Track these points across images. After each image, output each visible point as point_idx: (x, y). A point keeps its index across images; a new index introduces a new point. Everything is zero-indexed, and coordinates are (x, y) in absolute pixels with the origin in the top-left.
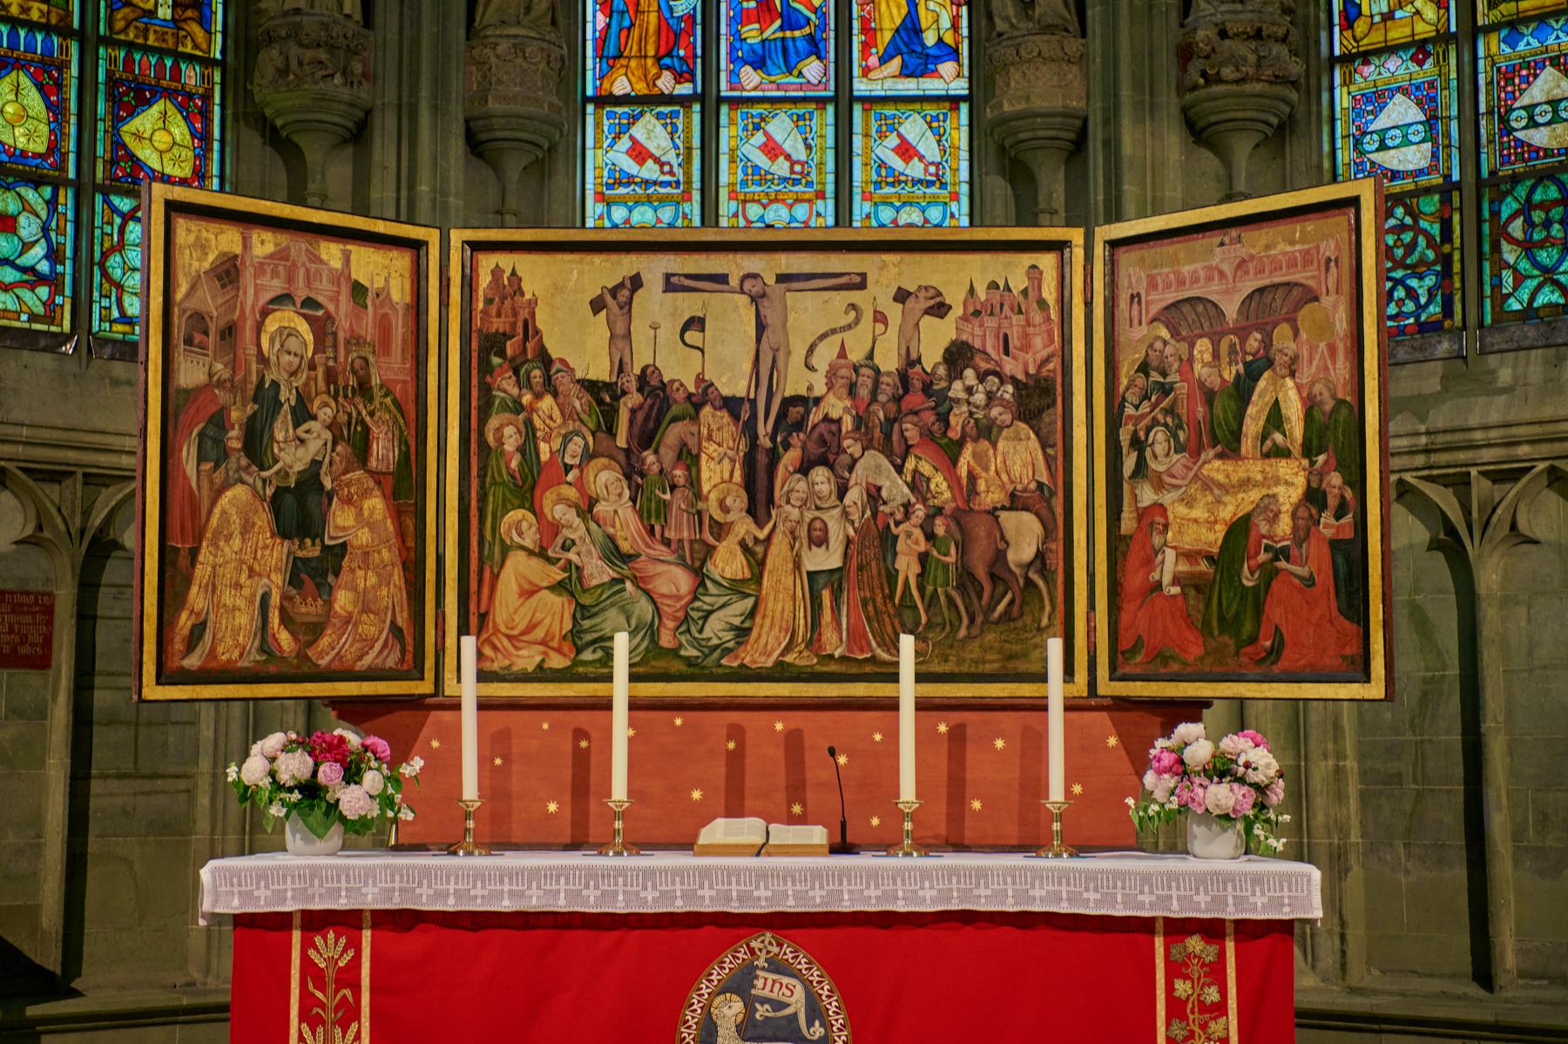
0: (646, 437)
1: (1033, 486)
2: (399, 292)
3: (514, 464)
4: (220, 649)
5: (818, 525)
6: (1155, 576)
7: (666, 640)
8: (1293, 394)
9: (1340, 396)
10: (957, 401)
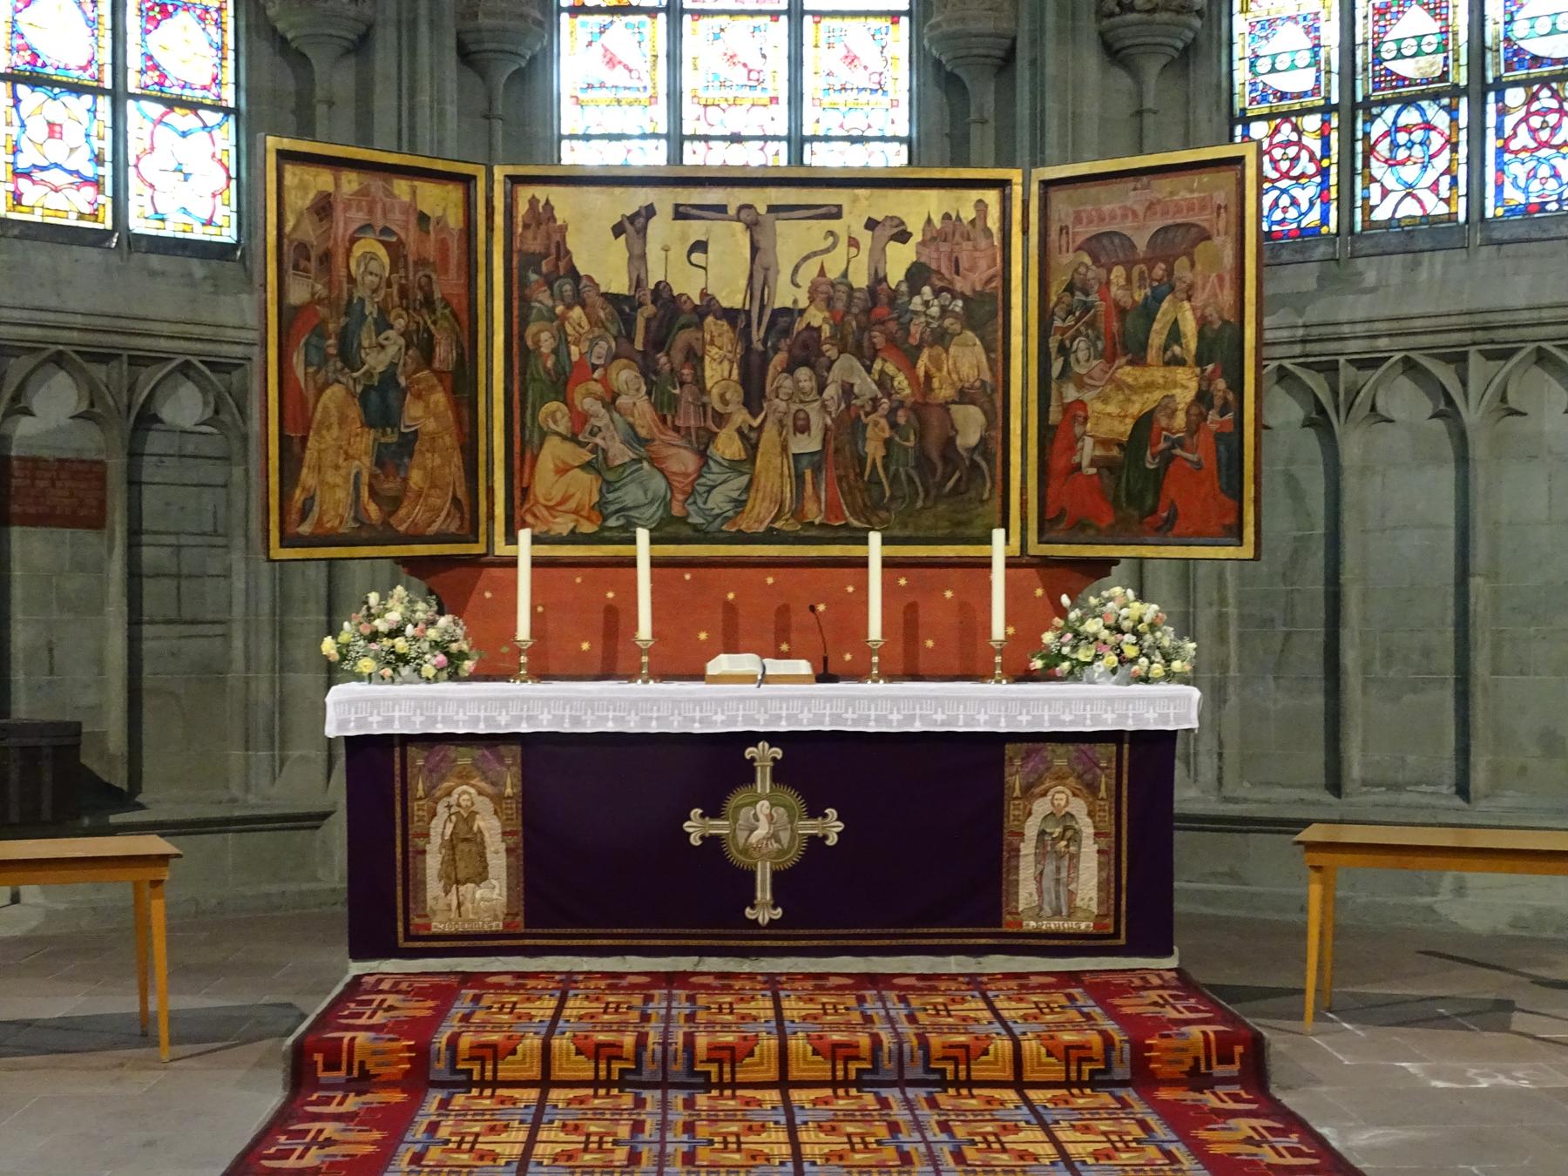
0: (658, 342)
1: (978, 384)
2: (455, 220)
3: (549, 364)
4: (325, 519)
5: (802, 415)
6: (1076, 459)
7: (677, 510)
8: (1189, 315)
9: (1226, 317)
10: (915, 313)
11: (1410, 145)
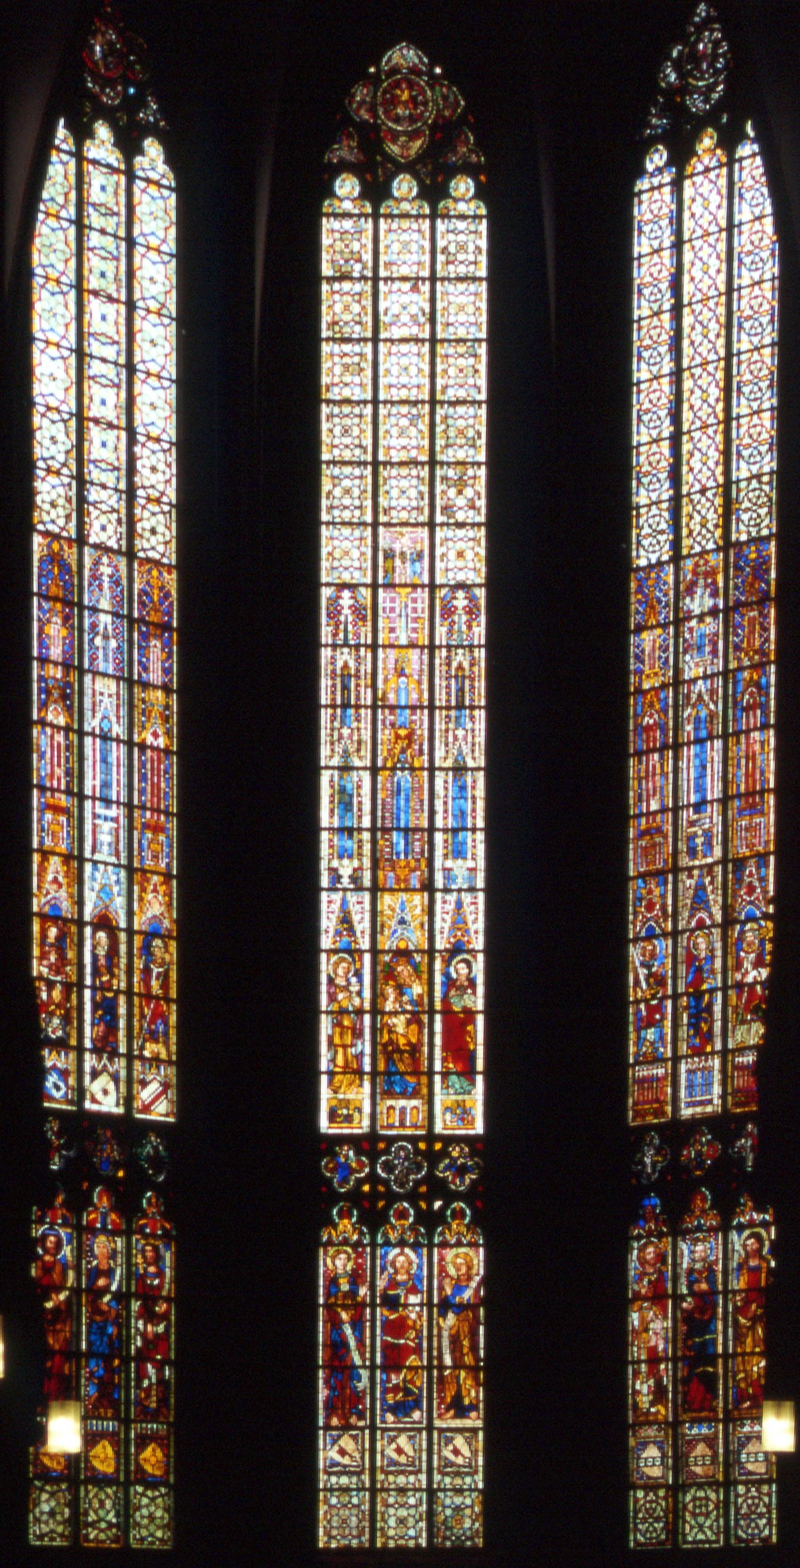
11: (700, 1507)
